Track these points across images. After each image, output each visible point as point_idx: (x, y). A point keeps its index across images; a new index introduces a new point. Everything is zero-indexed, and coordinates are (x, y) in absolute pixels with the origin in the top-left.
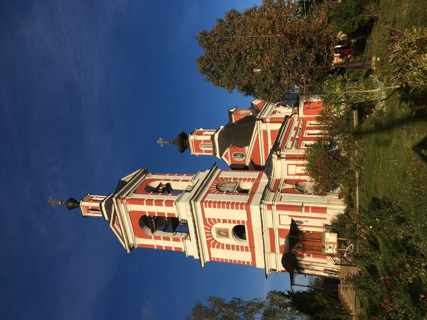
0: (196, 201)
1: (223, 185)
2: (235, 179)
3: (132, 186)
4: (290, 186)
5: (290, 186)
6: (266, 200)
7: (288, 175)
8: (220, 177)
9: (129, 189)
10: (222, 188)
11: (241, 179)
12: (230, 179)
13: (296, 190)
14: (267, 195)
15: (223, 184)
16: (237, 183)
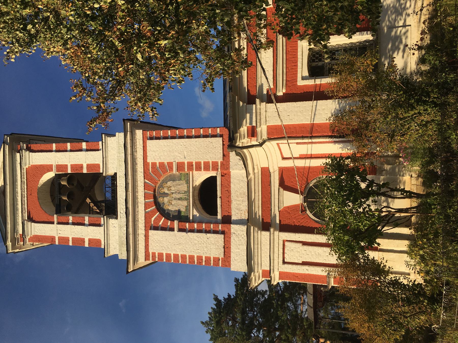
0: (137, 261)
1: (166, 191)
2: (180, 166)
3: (17, 199)
4: (293, 199)
5: (293, 199)
6: (256, 270)
7: (284, 158)
8: (150, 160)
9: (17, 210)
10: (166, 200)
11: (190, 165)
12: (170, 164)
13: (308, 212)
14: (256, 251)
15: (161, 186)
16: (188, 182)
